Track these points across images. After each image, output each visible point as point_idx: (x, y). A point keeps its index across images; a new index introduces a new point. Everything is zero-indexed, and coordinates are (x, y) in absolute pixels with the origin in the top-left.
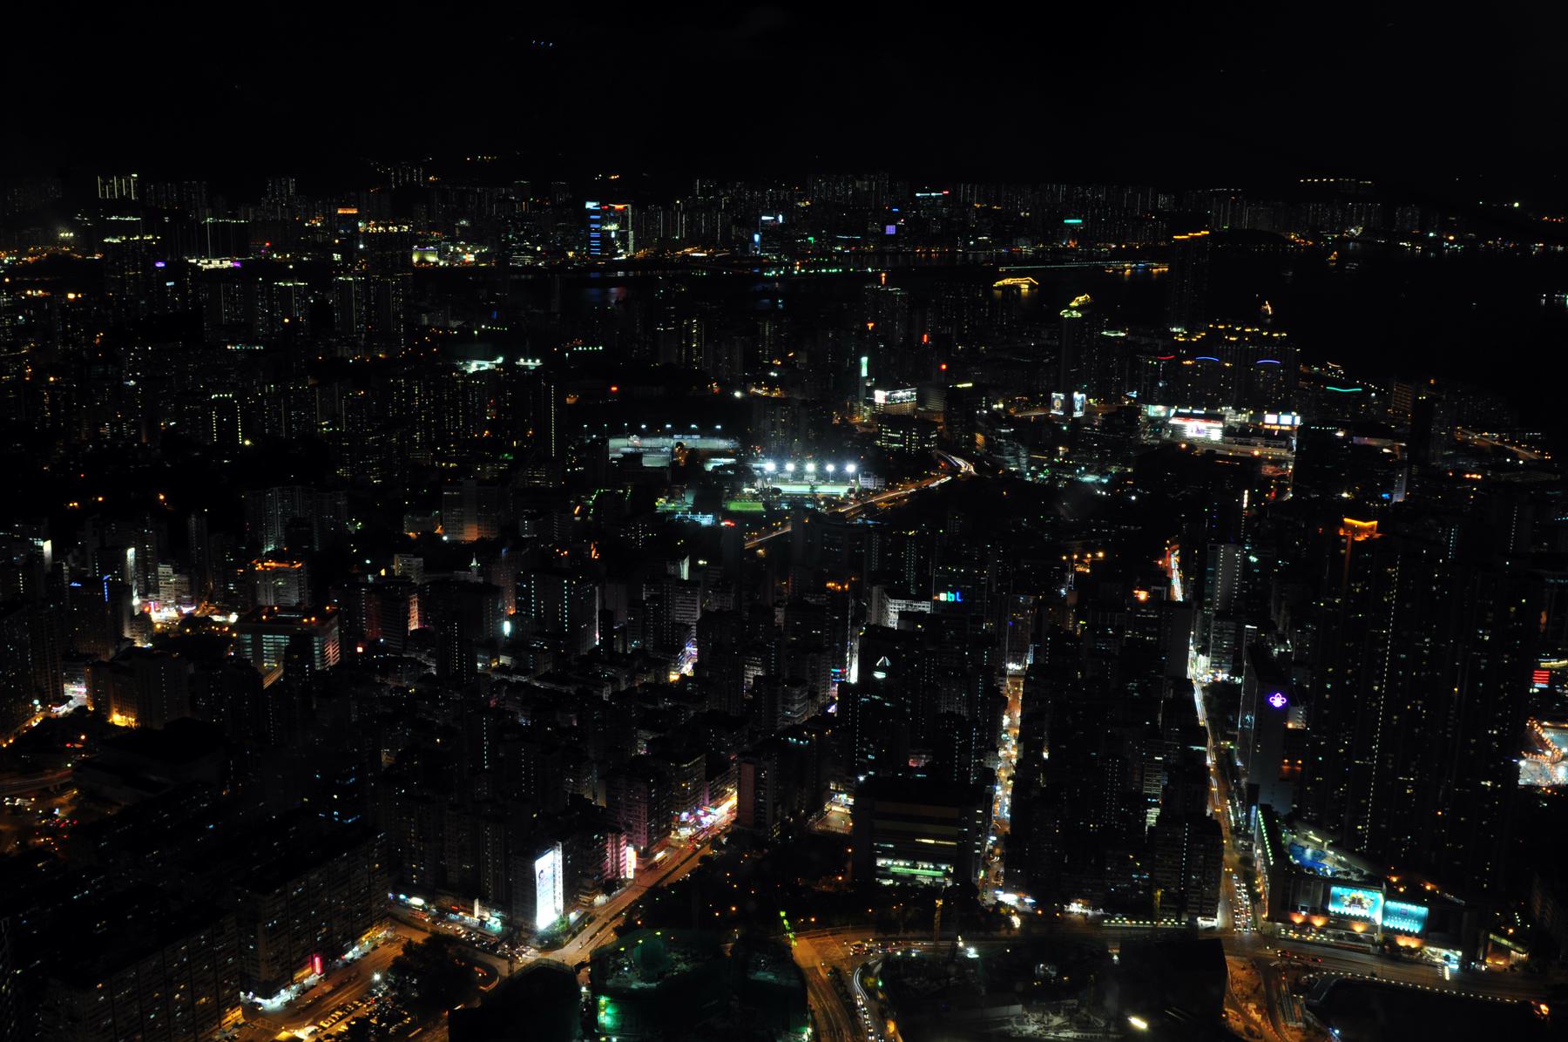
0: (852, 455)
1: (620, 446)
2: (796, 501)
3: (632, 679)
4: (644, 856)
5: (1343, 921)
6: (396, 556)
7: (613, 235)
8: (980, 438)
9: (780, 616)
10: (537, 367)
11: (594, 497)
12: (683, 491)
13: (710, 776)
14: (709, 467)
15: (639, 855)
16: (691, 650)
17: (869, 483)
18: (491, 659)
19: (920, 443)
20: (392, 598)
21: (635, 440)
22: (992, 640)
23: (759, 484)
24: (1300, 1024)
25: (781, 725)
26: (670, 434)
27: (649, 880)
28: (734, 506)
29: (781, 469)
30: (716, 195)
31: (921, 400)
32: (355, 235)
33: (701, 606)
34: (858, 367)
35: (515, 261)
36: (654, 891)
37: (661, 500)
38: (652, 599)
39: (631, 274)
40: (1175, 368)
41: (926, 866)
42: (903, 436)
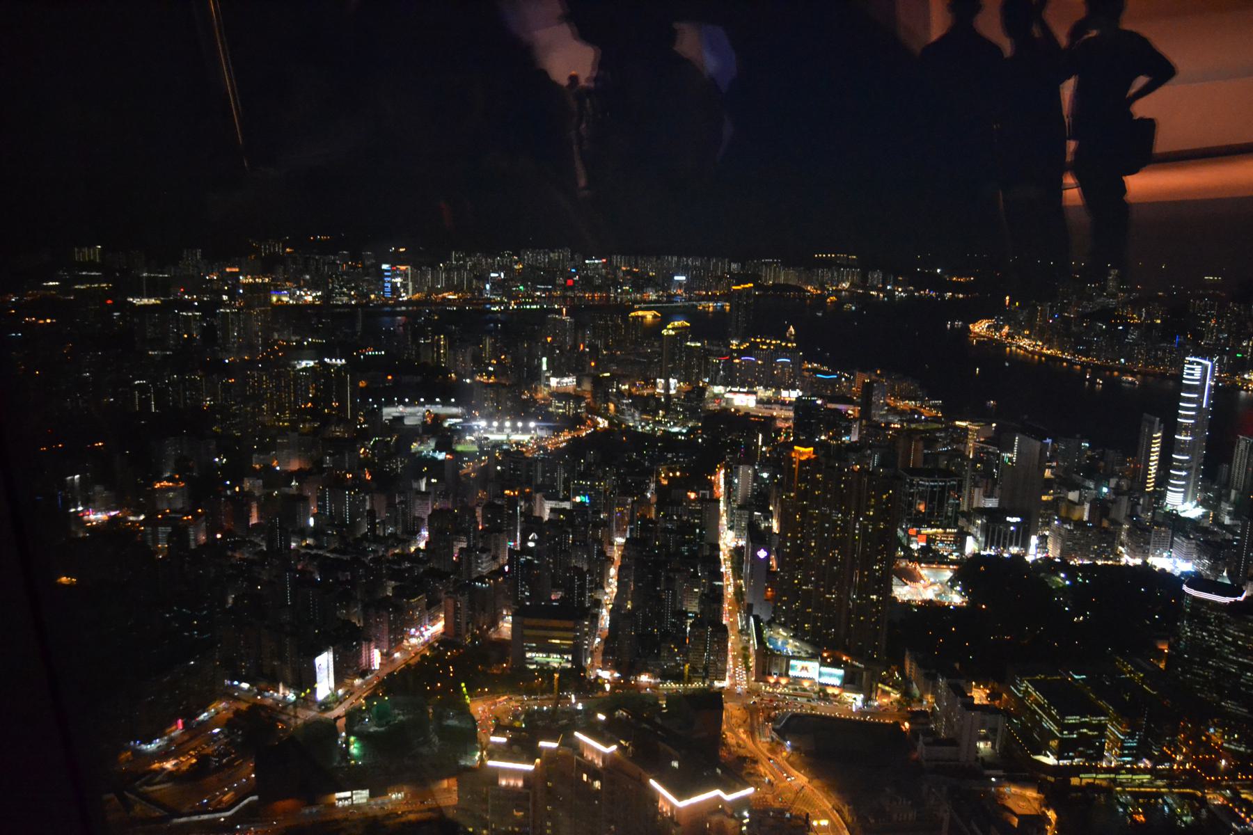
0: (534, 417)
1: (390, 412)
2: (497, 445)
3: (387, 551)
4: (386, 656)
5: (797, 680)
6: (245, 479)
7: (399, 285)
8: (612, 406)
9: (479, 512)
10: (342, 365)
11: (372, 443)
12: (429, 439)
13: (430, 606)
14: (446, 425)
15: (382, 654)
16: (425, 533)
17: (544, 434)
18: (302, 541)
19: (575, 409)
20: (241, 504)
21: (401, 408)
22: (606, 524)
23: (476, 434)
24: (769, 739)
25: (474, 576)
26: (423, 405)
27: (388, 670)
28: (459, 448)
29: (490, 425)
30: (465, 261)
31: (579, 384)
32: (237, 284)
33: (432, 507)
34: (540, 365)
35: (337, 300)
36: (390, 675)
37: (415, 444)
38: (401, 502)
39: (410, 308)
40: (729, 366)
41: (555, 656)
42: (565, 405)
